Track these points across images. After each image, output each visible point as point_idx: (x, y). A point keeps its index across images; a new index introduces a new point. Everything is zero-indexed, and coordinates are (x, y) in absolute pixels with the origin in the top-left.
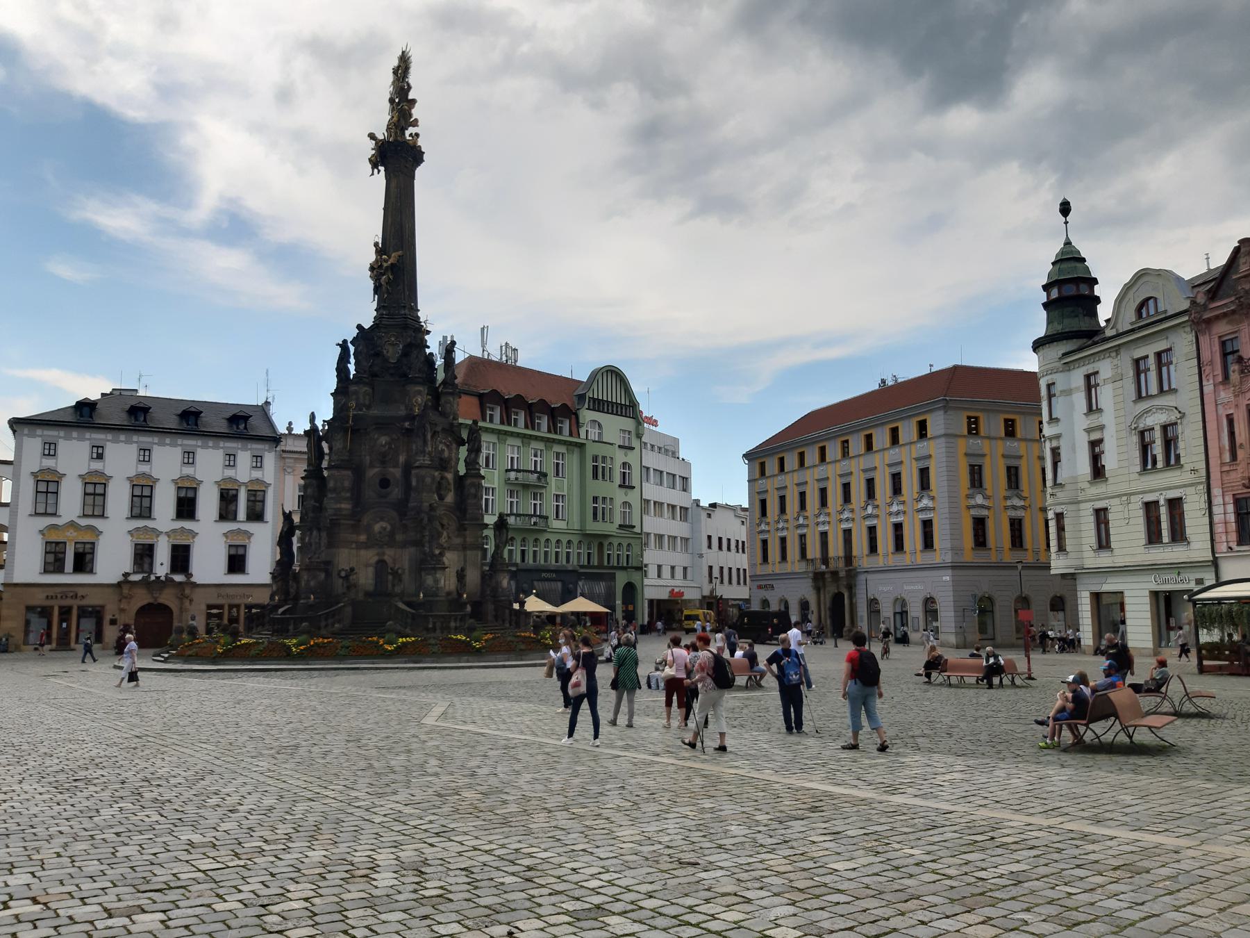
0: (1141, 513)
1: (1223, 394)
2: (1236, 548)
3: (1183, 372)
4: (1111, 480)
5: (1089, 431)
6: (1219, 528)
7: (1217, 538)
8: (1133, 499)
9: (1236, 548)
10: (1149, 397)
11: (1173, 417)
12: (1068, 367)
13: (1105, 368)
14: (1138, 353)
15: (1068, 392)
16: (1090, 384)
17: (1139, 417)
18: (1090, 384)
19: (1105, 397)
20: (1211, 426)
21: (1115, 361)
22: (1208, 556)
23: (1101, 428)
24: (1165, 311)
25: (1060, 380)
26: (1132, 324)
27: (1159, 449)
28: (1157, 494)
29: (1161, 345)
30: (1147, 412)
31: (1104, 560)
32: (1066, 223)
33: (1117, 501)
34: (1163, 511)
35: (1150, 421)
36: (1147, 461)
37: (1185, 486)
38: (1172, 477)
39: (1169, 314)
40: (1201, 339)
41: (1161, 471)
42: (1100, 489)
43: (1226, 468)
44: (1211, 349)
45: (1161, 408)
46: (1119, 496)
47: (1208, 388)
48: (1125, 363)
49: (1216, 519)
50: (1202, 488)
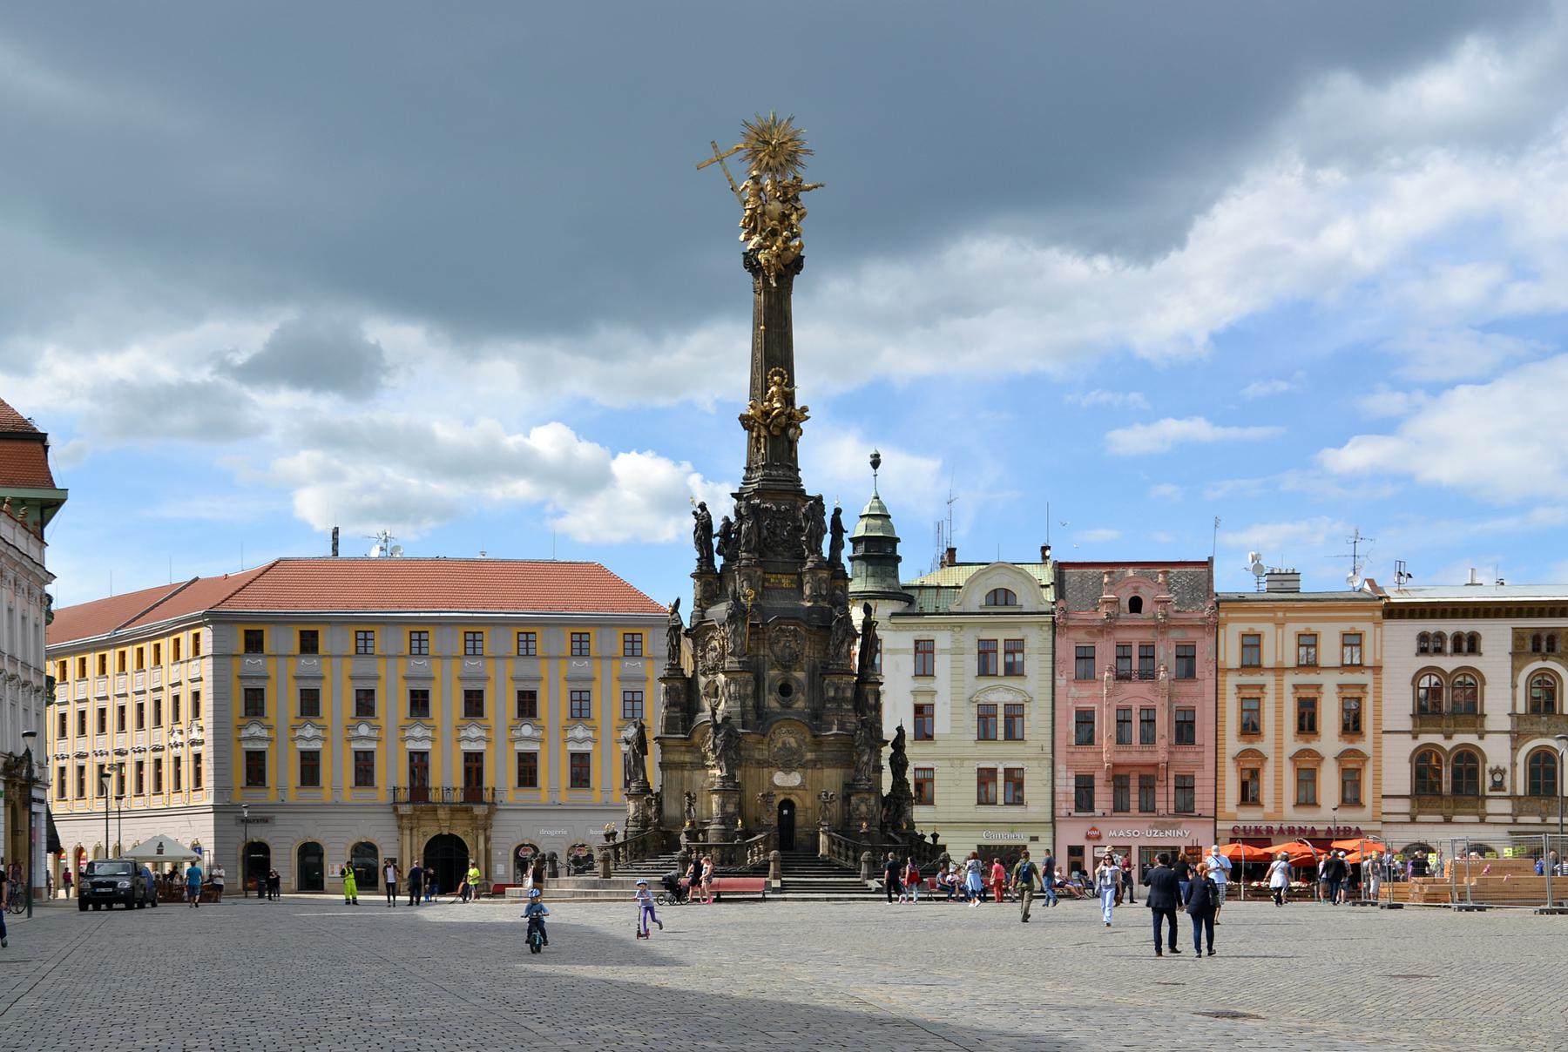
3: (1036, 662)
8: (966, 763)
11: (1019, 700)
12: (898, 628)
14: (987, 635)
15: (894, 652)
16: (924, 650)
18: (924, 650)
19: (942, 664)
27: (1000, 723)
29: (1015, 635)
33: (947, 763)
35: (992, 698)
36: (985, 735)
44: (1066, 649)
45: (1009, 689)
47: (1061, 682)
48: (969, 641)
50: (1048, 763)
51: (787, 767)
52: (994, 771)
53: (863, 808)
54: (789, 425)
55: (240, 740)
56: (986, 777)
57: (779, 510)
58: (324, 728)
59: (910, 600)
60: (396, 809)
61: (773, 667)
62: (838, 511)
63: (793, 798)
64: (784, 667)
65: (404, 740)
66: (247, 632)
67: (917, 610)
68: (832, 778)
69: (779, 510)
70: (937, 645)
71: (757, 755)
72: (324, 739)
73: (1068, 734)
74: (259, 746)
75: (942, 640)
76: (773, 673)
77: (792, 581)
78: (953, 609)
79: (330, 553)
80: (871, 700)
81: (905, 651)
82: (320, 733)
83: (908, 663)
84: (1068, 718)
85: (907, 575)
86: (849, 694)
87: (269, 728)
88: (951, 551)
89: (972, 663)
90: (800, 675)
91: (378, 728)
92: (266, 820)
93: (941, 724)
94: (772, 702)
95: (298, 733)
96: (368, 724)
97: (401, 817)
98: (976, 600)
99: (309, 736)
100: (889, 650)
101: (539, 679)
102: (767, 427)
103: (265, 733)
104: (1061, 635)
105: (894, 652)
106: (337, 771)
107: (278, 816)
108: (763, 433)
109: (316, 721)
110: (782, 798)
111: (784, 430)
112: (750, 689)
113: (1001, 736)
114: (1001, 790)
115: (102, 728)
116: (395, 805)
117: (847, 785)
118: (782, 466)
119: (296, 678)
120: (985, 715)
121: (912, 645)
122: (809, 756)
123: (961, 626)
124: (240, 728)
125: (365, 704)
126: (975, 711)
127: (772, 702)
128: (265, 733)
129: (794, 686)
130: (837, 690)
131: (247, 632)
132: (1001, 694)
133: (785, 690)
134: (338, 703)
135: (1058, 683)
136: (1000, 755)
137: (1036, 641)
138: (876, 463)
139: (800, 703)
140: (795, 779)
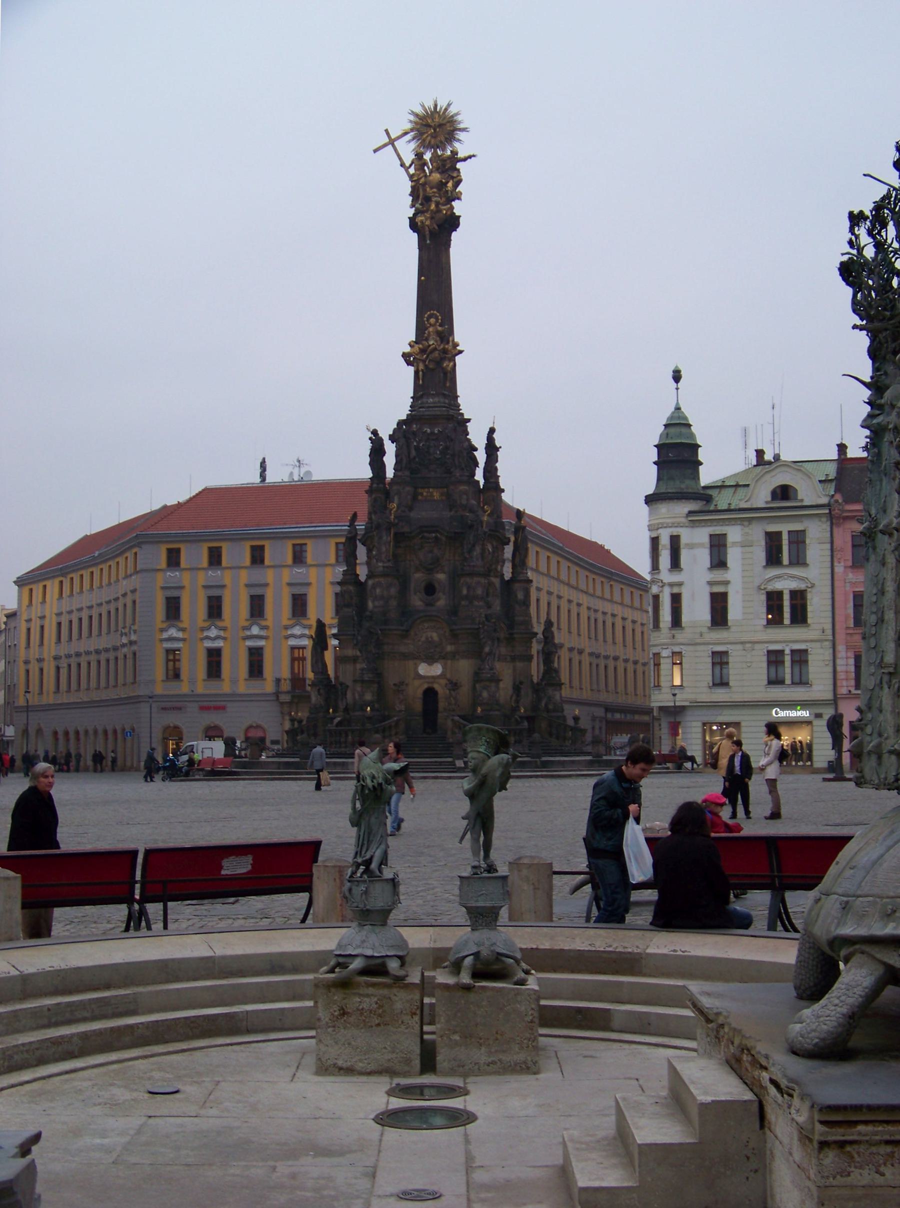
0: (765, 659)
1: (850, 575)
2: (854, 691)
3: (817, 551)
4: (733, 629)
5: (710, 583)
6: (841, 676)
7: (839, 683)
8: (757, 646)
9: (854, 691)
11: (802, 586)
12: (694, 524)
13: (734, 534)
14: (773, 528)
15: (691, 546)
16: (718, 545)
17: (770, 580)
18: (718, 545)
19: (733, 556)
20: (839, 598)
21: (746, 530)
22: (829, 696)
23: (727, 583)
24: (802, 500)
25: (687, 536)
26: (767, 502)
28: (784, 645)
29: (796, 526)
30: (778, 577)
31: (720, 695)
32: (677, 389)
33: (740, 647)
34: (788, 659)
35: (778, 586)
37: (812, 641)
38: (798, 633)
39: (805, 503)
40: (835, 530)
41: (787, 626)
42: (720, 635)
43: (851, 631)
45: (793, 577)
46: (742, 643)
47: (839, 569)
48: (757, 533)
49: (839, 668)
50: (828, 644)
52: (781, 652)
53: (485, 694)
54: (442, 359)
55: (162, 640)
56: (775, 658)
57: (432, 433)
58: (224, 629)
59: (708, 499)
60: (278, 696)
62: (492, 431)
63: (436, 687)
65: (287, 637)
66: (294, 545)
67: (712, 508)
68: (465, 667)
69: (432, 433)
70: (730, 539)
71: (403, 649)
72: (224, 639)
73: (847, 617)
74: (176, 645)
75: (734, 534)
76: (418, 575)
77: (442, 494)
79: (258, 480)
80: (520, 596)
81: (701, 545)
82: (222, 633)
83: (704, 556)
84: (846, 602)
85: (707, 476)
86: (479, 591)
87: (183, 630)
88: (760, 453)
89: (760, 554)
90: (441, 576)
91: (224, 629)
92: (180, 709)
93: (734, 612)
94: (417, 601)
95: (205, 634)
96: (258, 625)
97: (282, 704)
98: (762, 496)
99: (214, 637)
100: (687, 545)
101: (267, 585)
102: (424, 361)
103: (180, 635)
104: (838, 525)
105: (691, 546)
106: (235, 665)
107: (229, 705)
108: (421, 367)
109: (220, 624)
110: (426, 686)
111: (439, 363)
112: (393, 591)
113: (787, 621)
114: (788, 670)
115: (100, 634)
116: (277, 694)
117: (476, 674)
118: (437, 395)
119: (247, 586)
120: (773, 600)
121: (706, 540)
122: (449, 648)
123: (750, 520)
124: (162, 630)
125: (257, 607)
126: (763, 598)
127: (417, 601)
128: (180, 635)
129: (437, 586)
130: (469, 588)
131: (294, 545)
132: (786, 581)
133: (430, 589)
134: (236, 607)
135: (836, 570)
136: (788, 638)
137: (816, 533)
138: (677, 376)
139: (442, 602)
140: (436, 670)
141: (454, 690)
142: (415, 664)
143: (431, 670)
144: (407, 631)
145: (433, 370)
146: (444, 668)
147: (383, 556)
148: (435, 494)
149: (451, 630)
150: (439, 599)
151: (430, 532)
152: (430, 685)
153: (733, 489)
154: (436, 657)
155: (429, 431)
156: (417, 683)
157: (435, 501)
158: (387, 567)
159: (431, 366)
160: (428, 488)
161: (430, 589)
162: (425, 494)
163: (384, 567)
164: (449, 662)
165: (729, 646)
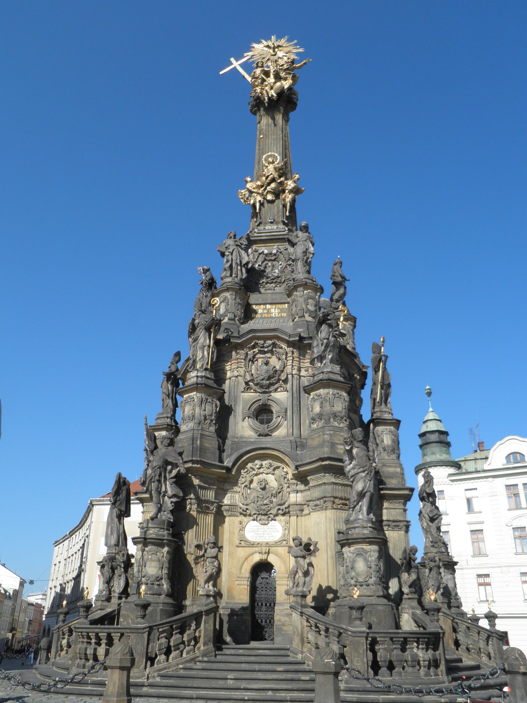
8: (511, 569)
10: (521, 508)
51: (265, 515)
53: (361, 565)
61: (248, 387)
63: (272, 559)
64: (262, 387)
67: (464, 471)
68: (320, 525)
77: (282, 311)
78: (486, 467)
102: (262, 194)
110: (257, 558)
111: (278, 193)
122: (293, 498)
138: (429, 394)
141: (304, 557)
142: (241, 523)
143: (265, 534)
144: (229, 470)
145: (271, 202)
146: (287, 528)
147: (198, 366)
148: (273, 311)
149: (297, 467)
150: (278, 427)
151: (265, 339)
152: (264, 557)
153: (474, 461)
154: (274, 511)
155: (266, 252)
156: (242, 552)
157: (271, 317)
158: (202, 377)
159: (270, 197)
160: (265, 304)
161: (262, 413)
162: (260, 311)
163: (197, 377)
164: (293, 518)
165: (489, 569)
